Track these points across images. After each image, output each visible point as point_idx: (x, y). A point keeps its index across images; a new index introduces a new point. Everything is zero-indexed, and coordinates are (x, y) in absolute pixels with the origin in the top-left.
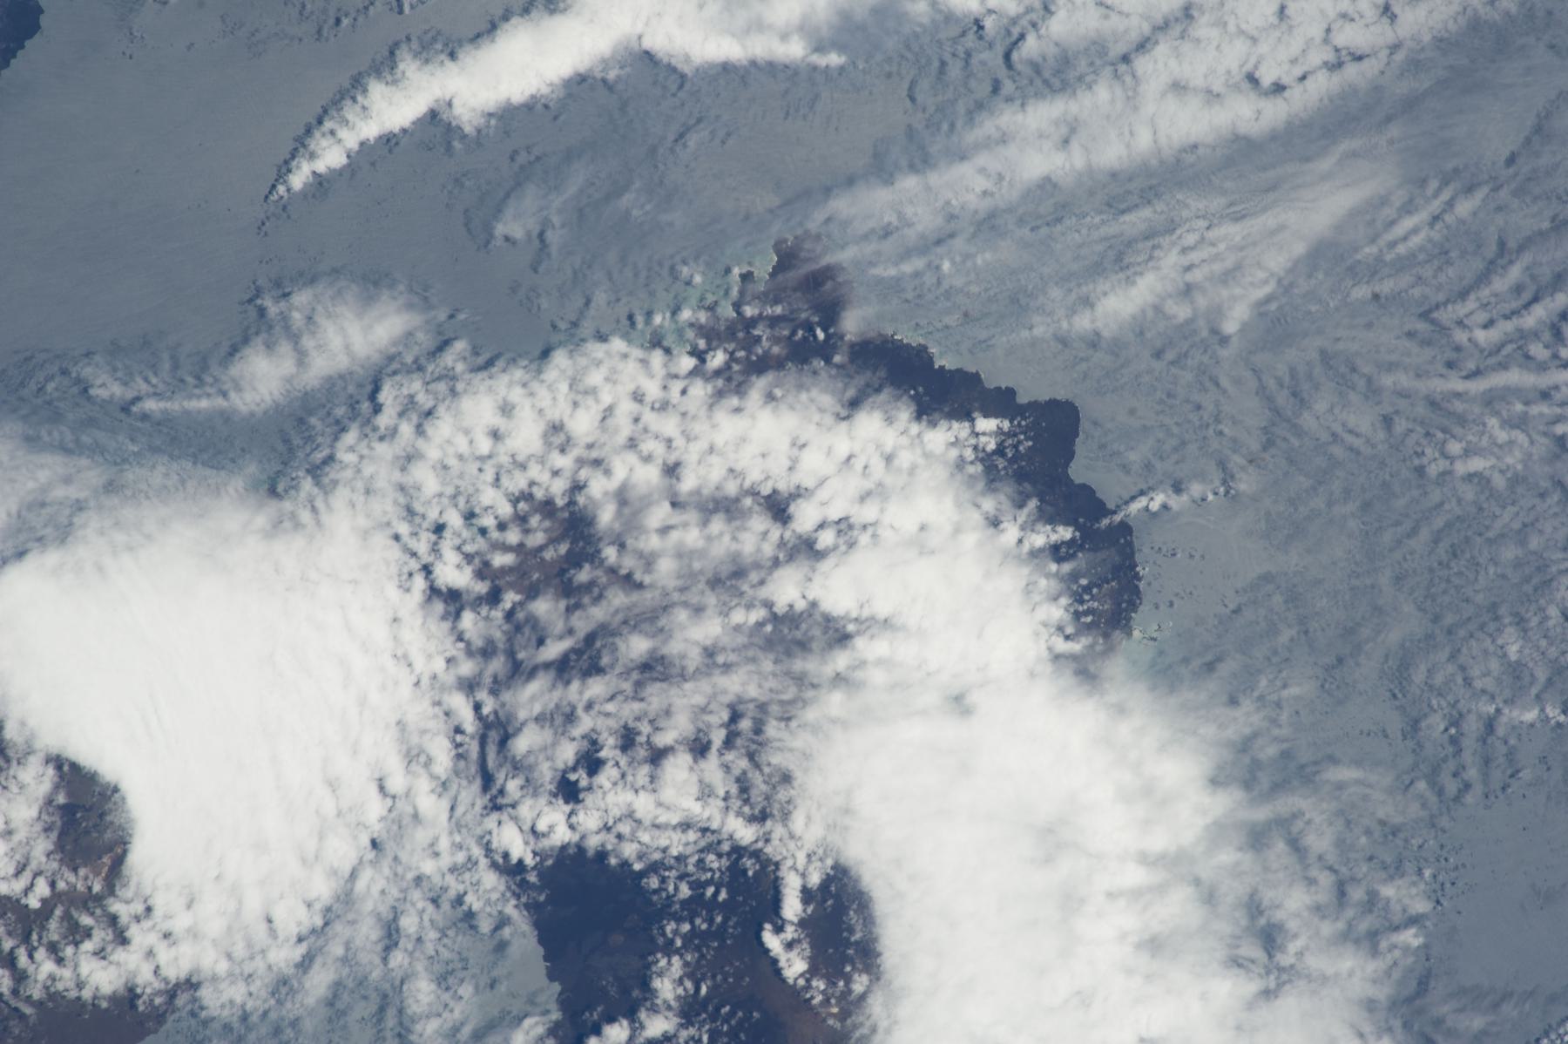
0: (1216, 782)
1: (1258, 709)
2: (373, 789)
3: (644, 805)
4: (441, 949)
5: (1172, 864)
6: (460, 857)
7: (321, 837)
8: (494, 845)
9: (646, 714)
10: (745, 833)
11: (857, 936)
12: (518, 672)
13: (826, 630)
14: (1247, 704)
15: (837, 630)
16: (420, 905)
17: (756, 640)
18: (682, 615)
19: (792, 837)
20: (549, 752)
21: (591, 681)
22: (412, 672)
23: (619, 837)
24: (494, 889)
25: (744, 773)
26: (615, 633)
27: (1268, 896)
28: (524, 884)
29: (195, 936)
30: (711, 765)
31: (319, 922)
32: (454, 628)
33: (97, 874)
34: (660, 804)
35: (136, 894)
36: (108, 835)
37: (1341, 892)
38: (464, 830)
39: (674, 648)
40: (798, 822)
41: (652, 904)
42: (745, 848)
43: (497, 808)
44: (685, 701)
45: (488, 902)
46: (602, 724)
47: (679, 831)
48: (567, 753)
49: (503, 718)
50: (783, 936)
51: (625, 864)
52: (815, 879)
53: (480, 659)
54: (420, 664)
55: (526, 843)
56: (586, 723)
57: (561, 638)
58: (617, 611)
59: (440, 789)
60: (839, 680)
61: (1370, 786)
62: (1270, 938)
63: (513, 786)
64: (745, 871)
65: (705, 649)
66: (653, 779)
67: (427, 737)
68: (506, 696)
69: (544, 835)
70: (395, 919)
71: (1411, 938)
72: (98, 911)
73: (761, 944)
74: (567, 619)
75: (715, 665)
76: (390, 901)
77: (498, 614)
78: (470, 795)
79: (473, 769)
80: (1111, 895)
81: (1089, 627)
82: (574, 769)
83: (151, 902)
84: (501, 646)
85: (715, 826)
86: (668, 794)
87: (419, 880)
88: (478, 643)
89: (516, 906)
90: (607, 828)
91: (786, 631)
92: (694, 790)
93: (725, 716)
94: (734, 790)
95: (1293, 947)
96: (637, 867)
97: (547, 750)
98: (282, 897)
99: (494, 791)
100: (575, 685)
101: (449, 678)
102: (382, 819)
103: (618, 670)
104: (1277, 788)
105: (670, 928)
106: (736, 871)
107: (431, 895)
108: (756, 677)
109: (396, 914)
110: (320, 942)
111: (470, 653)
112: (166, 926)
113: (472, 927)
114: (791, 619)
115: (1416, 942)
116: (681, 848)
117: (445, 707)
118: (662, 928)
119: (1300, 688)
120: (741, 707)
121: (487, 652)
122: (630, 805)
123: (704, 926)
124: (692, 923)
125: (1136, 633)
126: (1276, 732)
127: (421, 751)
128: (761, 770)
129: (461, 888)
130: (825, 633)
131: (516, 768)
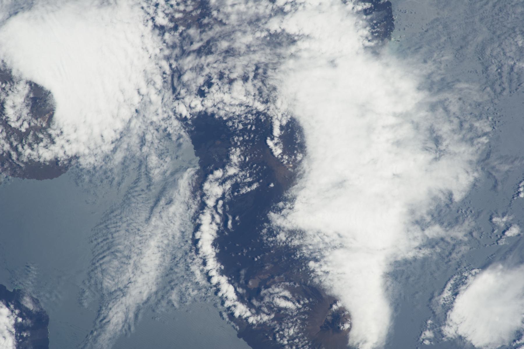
0: (419, 89)
1: (434, 64)
2: (136, 93)
3: (227, 98)
4: (160, 146)
5: (404, 116)
6: (166, 115)
7: (119, 109)
8: (177, 111)
9: (227, 67)
10: (261, 107)
11: (299, 141)
12: (184, 53)
13: (287, 39)
14: (430, 63)
15: (291, 39)
16: (152, 131)
17: (264, 42)
18: (239, 34)
19: (277, 108)
20: (195, 80)
21: (208, 56)
22: (148, 53)
23: (219, 108)
24: (177, 126)
25: (260, 87)
26: (216, 40)
27: (436, 126)
28: (187, 124)
29: (77, 141)
30: (249, 85)
31: (119, 137)
32: (162, 39)
33: (44, 120)
34: (232, 98)
35: (57, 127)
36: (48, 108)
37: (461, 125)
38: (167, 107)
39: (236, 45)
40: (279, 103)
41: (229, 131)
42: (261, 112)
43: (178, 99)
44: (240, 63)
45: (175, 130)
46: (212, 71)
47: (239, 106)
48: (201, 80)
49: (179, 69)
50: (274, 141)
51: (221, 118)
52: (284, 122)
53: (171, 49)
54: (151, 51)
55: (188, 111)
56: (207, 71)
57: (198, 42)
58: (217, 33)
59: (158, 93)
60: (292, 56)
61: (471, 89)
62: (437, 140)
63: (183, 92)
64: (261, 120)
65: (247, 45)
66: (230, 89)
67: (154, 75)
68: (180, 62)
69: (193, 108)
70: (144, 136)
71: (484, 140)
72: (45, 133)
73: (266, 144)
74: (200, 35)
75: (250, 51)
76: (142, 130)
77: (177, 34)
78: (168, 95)
79: (169, 86)
80: (384, 127)
81: (376, 37)
82: (203, 86)
83: (62, 130)
84: (178, 45)
85: (250, 105)
86: (235, 94)
87: (152, 123)
88: (171, 44)
89: (184, 132)
90: (214, 106)
91: (274, 39)
92: (244, 93)
93: (254, 68)
94: (257, 93)
95: (445, 144)
96: (225, 118)
97: (194, 80)
98: (106, 129)
99: (176, 93)
100: (203, 58)
101: (161, 56)
102: (139, 103)
103: (218, 53)
104: (440, 90)
105: (236, 139)
106: (258, 120)
107: (156, 128)
108: (264, 55)
109: (144, 134)
110: (119, 143)
111: (168, 47)
112: (68, 138)
113: (170, 139)
114: (276, 35)
115: (486, 141)
116: (239, 112)
117: (160, 65)
118: (233, 139)
119: (448, 57)
120: (259, 65)
121: (174, 47)
122: (222, 98)
123: (247, 138)
124: (243, 137)
125: (393, 39)
126: (440, 72)
127: (152, 80)
128: (266, 86)
129: (166, 126)
130: (287, 40)
131: (184, 86)
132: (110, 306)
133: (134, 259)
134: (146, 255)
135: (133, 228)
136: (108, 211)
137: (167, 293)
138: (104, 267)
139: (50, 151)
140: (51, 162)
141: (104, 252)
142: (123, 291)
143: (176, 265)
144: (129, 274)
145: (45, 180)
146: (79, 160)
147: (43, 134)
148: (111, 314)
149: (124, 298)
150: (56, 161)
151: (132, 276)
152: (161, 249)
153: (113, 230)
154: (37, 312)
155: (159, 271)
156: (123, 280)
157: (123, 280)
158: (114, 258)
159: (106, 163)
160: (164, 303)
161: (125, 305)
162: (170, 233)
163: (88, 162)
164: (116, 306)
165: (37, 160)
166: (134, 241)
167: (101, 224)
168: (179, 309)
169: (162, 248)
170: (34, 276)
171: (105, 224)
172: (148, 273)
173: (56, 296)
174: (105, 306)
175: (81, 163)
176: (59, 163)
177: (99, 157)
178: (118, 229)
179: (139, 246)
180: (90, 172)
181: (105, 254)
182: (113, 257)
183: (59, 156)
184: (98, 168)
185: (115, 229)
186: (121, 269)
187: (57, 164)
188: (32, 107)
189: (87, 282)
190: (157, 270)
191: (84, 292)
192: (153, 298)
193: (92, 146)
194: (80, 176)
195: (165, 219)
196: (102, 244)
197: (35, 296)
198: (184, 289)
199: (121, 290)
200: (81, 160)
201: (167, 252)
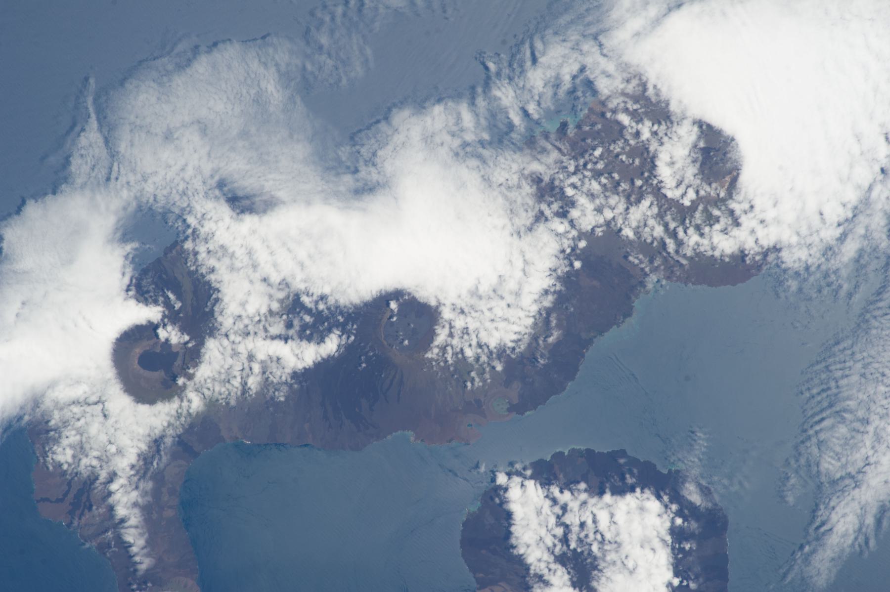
33: (722, 187)
35: (745, 198)
36: (729, 165)
72: (723, 208)
83: (753, 203)
98: (828, 201)
112: (761, 216)
132: (832, 504)
136: (832, 342)
138: (822, 436)
139: (731, 239)
140: (732, 256)
141: (822, 411)
145: (722, 287)
146: (780, 255)
147: (720, 209)
148: (834, 517)
150: (742, 255)
154: (707, 509)
159: (827, 260)
163: (796, 257)
165: (710, 253)
167: (818, 362)
170: (703, 449)
173: (740, 483)
174: (824, 503)
175: (784, 259)
176: (747, 259)
177: (815, 249)
180: (800, 275)
181: (824, 415)
183: (747, 247)
184: (813, 269)
187: (744, 261)
188: (703, 164)
189: (792, 462)
191: (788, 478)
193: (804, 231)
194: (782, 281)
196: (819, 398)
197: (704, 483)
200: (784, 254)
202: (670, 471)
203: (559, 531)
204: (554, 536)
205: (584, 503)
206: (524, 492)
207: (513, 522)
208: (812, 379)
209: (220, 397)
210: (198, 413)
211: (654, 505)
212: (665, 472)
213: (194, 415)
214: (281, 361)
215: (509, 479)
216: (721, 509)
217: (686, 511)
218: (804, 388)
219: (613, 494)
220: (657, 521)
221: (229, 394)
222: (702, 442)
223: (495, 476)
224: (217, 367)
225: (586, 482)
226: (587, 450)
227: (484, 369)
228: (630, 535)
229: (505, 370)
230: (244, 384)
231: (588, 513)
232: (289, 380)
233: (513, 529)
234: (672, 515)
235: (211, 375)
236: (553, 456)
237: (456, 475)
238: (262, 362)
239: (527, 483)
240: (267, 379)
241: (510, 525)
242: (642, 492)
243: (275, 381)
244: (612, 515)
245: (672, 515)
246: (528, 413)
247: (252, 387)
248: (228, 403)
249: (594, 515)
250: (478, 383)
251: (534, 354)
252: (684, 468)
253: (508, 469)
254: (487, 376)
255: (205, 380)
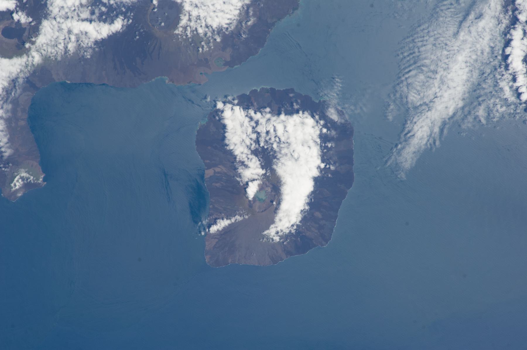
132: (415, 120)
133: (440, 74)
134: (453, 70)
135: (440, 42)
137: (474, 108)
138: (410, 81)
141: (410, 66)
142: (428, 106)
143: (484, 80)
144: (435, 89)
148: (416, 128)
149: (429, 112)
151: (438, 90)
152: (468, 64)
153: (420, 44)
154: (341, 123)
155: (466, 86)
156: (429, 95)
157: (429, 95)
158: (419, 73)
160: (470, 119)
161: (431, 119)
162: (479, 49)
164: (421, 120)
166: (441, 55)
167: (408, 37)
168: (487, 124)
169: (470, 63)
170: (339, 88)
171: (411, 38)
172: (455, 88)
173: (361, 108)
174: (410, 120)
178: (425, 43)
179: (446, 61)
181: (411, 68)
182: (420, 71)
185: (421, 43)
186: (427, 84)
189: (392, 96)
190: (464, 85)
191: (389, 105)
192: (459, 113)
195: (474, 33)
196: (408, 59)
197: (340, 108)
198: (491, 106)
199: (427, 105)
201: (475, 67)
202: (320, 101)
203: (254, 136)
204: (251, 139)
205: (269, 120)
206: (233, 113)
207: (226, 130)
208: (404, 47)
209: (51, 55)
210: (38, 64)
211: (310, 121)
212: (318, 102)
213: (36, 65)
214: (88, 34)
215: (224, 105)
216: (350, 124)
217: (329, 125)
218: (399, 53)
219: (286, 114)
220: (312, 131)
221: (57, 53)
222: (338, 85)
223: (216, 103)
224: (49, 37)
225: (270, 107)
226: (271, 88)
227: (210, 41)
228: (296, 138)
229: (222, 41)
230: (66, 48)
231: (271, 126)
232: (93, 45)
233: (226, 134)
234: (320, 127)
235: (46, 42)
236: (251, 92)
237: (193, 103)
238: (76, 35)
239: (235, 108)
240: (80, 45)
241: (225, 132)
242: (303, 113)
243: (84, 46)
244: (285, 127)
245: (320, 127)
246: (236, 66)
247: (71, 49)
248: (56, 59)
249: (275, 127)
250: (206, 49)
251: (239, 32)
252: (328, 99)
253: (224, 100)
254: (211, 44)
255: (42, 45)
